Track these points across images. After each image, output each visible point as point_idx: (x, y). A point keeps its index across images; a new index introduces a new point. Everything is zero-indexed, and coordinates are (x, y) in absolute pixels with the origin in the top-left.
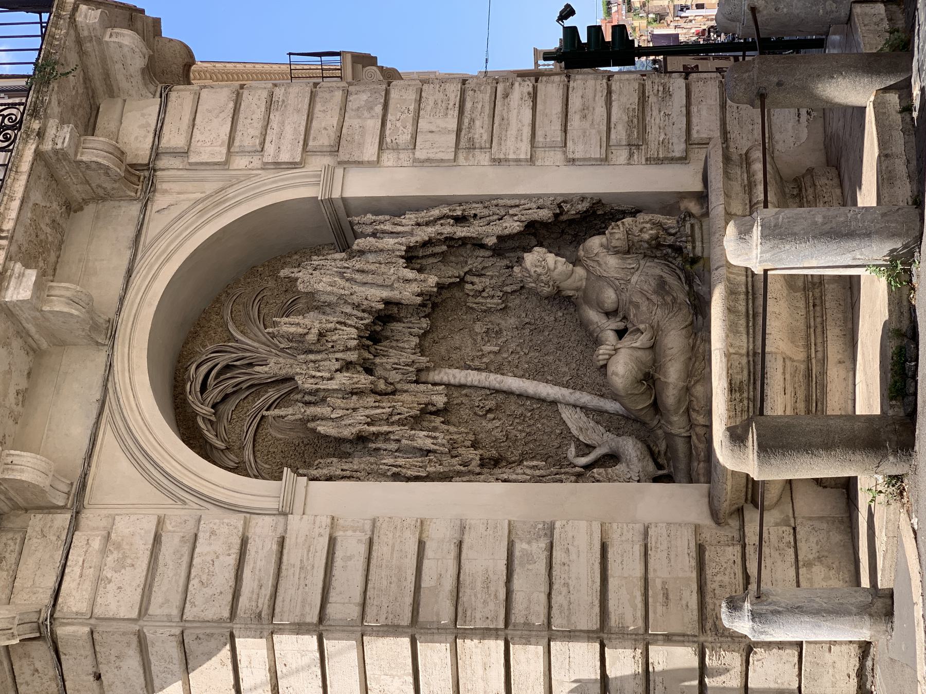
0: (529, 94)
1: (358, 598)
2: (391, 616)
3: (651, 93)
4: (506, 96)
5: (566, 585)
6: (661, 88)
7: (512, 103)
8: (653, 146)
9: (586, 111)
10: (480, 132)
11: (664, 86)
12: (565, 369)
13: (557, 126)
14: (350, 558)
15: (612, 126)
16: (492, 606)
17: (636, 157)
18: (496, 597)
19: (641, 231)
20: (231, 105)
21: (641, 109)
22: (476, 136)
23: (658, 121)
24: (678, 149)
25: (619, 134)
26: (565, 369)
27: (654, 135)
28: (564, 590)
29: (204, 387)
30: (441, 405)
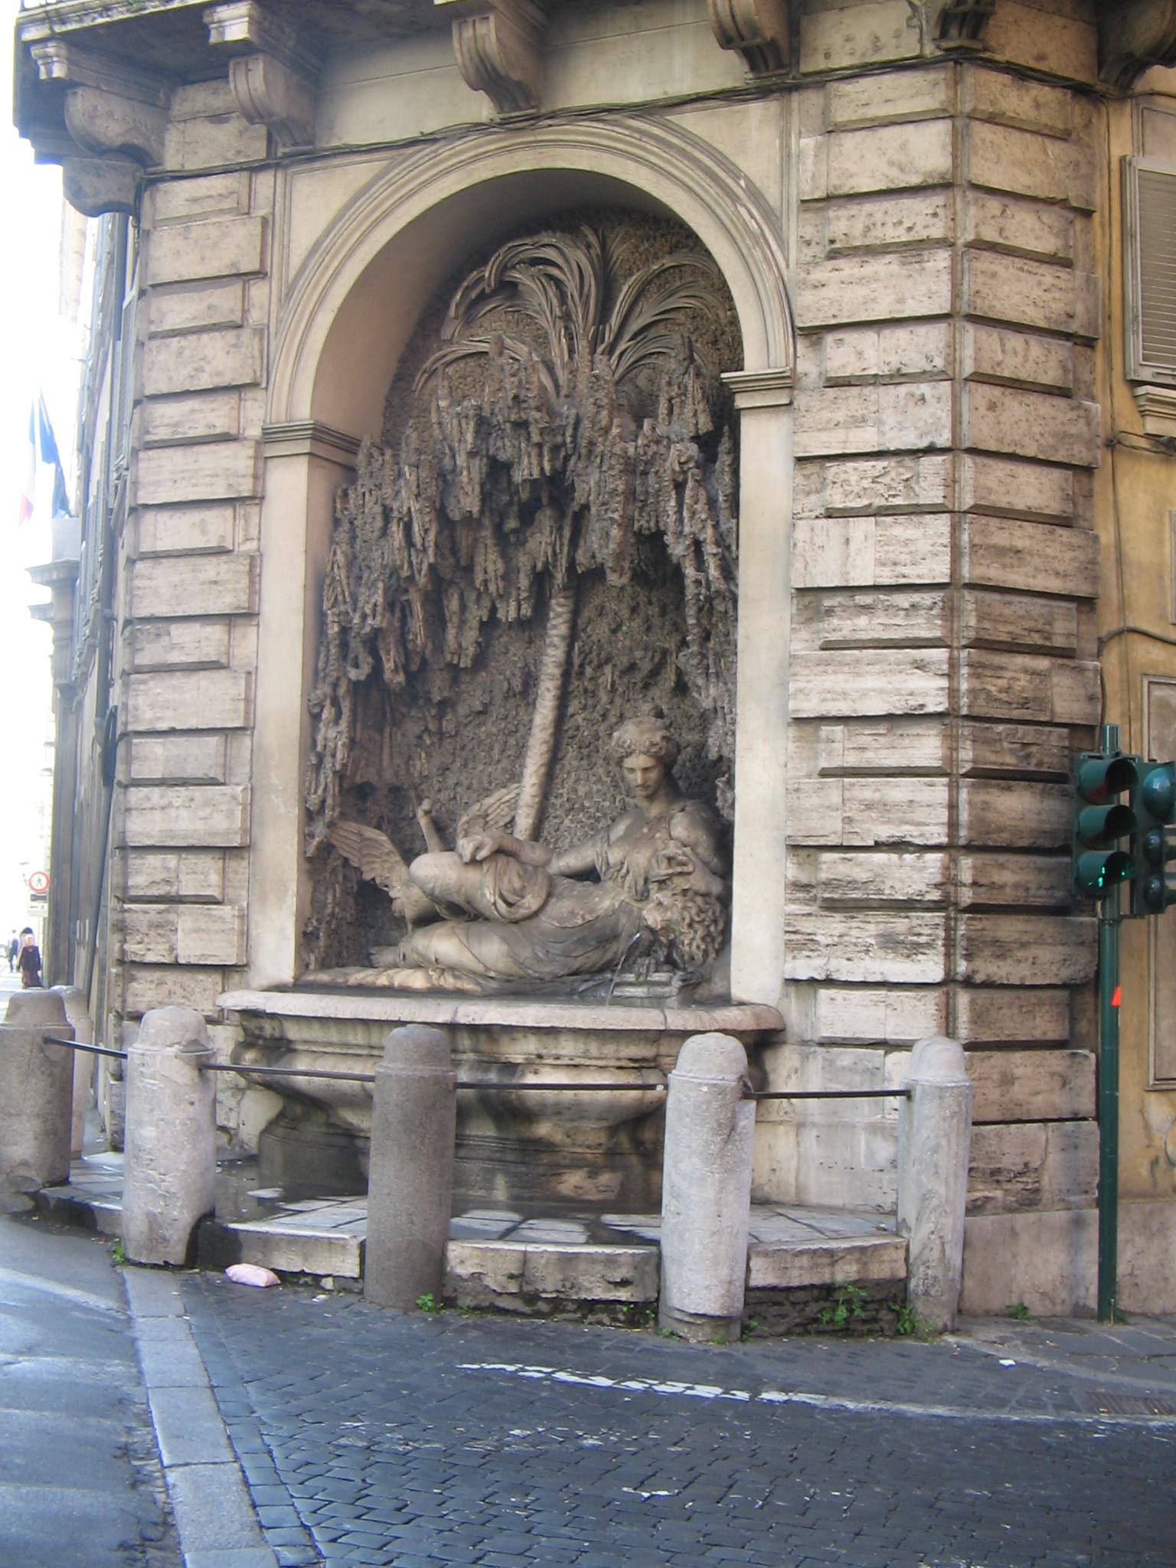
0: (922, 706)
1: (163, 546)
2: (139, 592)
3: (915, 922)
4: (920, 666)
5: (170, 805)
6: (923, 940)
7: (903, 676)
8: (807, 926)
9: (882, 808)
10: (844, 626)
11: (929, 945)
12: (582, 790)
13: (852, 760)
14: (204, 532)
15: (849, 855)
16: (149, 715)
17: (800, 895)
18: (159, 718)
19: (660, 904)
20: (915, 180)
21: (885, 904)
22: (835, 622)
23: (854, 933)
24: (805, 968)
25: (831, 866)
26: (582, 790)
27: (834, 926)
28: (163, 802)
29: (535, 262)
30: (500, 615)
